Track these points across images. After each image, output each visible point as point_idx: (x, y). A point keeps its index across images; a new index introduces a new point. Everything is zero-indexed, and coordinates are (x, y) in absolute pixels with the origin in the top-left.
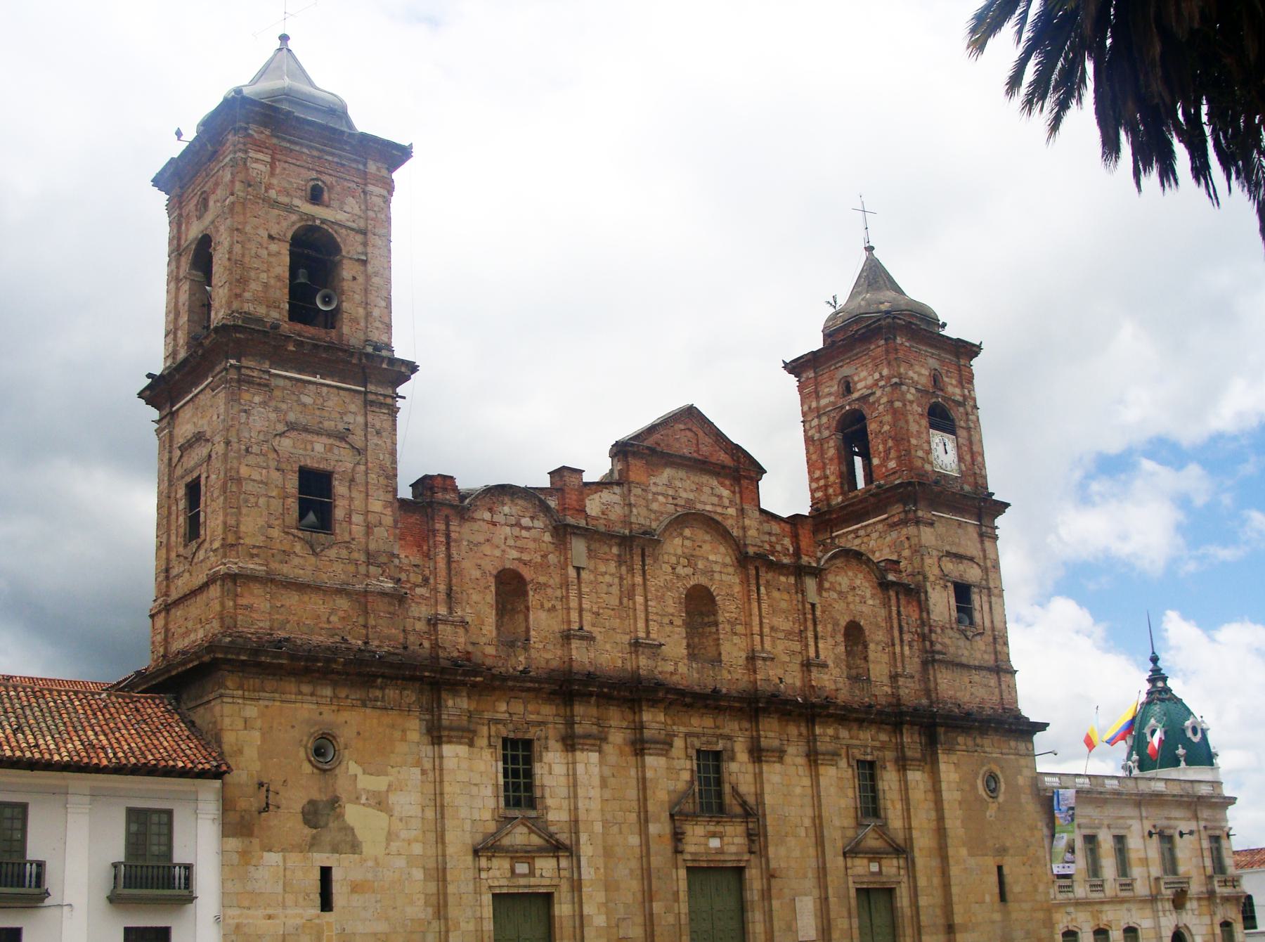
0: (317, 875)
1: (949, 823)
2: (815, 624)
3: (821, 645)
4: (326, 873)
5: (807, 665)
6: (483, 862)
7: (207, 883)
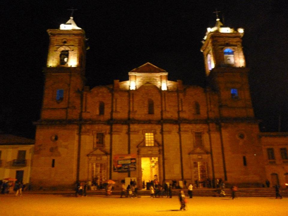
0: (52, 161)
1: (224, 146)
2: (182, 103)
3: (183, 107)
4: (54, 160)
5: (179, 112)
6: (90, 157)
7: (29, 163)
